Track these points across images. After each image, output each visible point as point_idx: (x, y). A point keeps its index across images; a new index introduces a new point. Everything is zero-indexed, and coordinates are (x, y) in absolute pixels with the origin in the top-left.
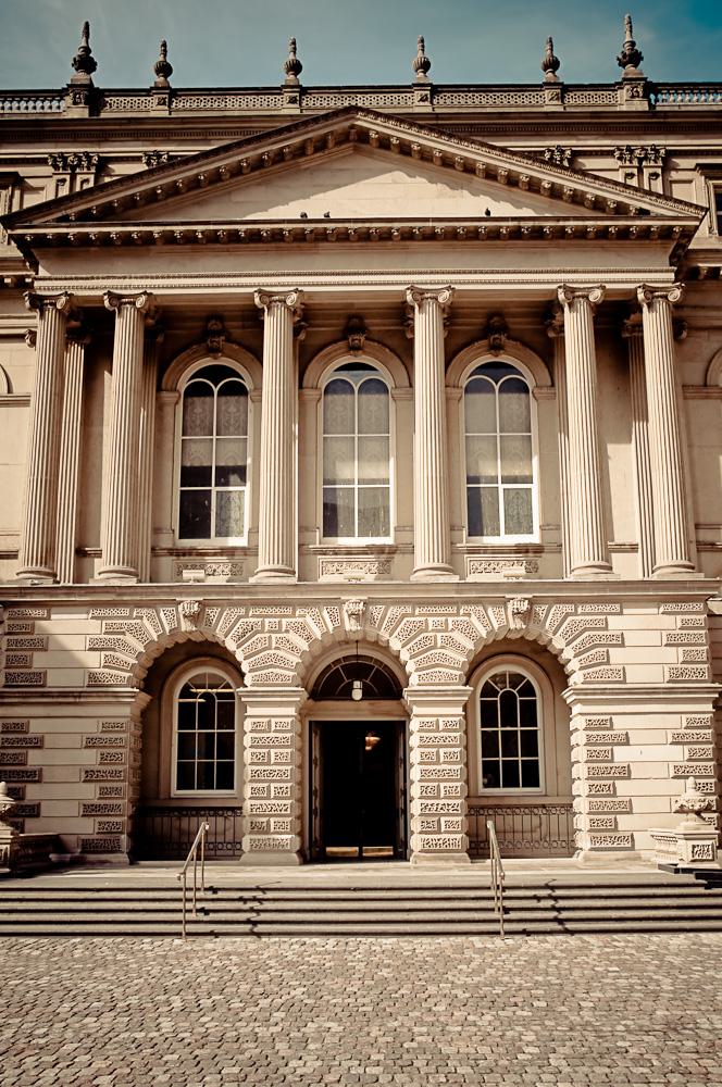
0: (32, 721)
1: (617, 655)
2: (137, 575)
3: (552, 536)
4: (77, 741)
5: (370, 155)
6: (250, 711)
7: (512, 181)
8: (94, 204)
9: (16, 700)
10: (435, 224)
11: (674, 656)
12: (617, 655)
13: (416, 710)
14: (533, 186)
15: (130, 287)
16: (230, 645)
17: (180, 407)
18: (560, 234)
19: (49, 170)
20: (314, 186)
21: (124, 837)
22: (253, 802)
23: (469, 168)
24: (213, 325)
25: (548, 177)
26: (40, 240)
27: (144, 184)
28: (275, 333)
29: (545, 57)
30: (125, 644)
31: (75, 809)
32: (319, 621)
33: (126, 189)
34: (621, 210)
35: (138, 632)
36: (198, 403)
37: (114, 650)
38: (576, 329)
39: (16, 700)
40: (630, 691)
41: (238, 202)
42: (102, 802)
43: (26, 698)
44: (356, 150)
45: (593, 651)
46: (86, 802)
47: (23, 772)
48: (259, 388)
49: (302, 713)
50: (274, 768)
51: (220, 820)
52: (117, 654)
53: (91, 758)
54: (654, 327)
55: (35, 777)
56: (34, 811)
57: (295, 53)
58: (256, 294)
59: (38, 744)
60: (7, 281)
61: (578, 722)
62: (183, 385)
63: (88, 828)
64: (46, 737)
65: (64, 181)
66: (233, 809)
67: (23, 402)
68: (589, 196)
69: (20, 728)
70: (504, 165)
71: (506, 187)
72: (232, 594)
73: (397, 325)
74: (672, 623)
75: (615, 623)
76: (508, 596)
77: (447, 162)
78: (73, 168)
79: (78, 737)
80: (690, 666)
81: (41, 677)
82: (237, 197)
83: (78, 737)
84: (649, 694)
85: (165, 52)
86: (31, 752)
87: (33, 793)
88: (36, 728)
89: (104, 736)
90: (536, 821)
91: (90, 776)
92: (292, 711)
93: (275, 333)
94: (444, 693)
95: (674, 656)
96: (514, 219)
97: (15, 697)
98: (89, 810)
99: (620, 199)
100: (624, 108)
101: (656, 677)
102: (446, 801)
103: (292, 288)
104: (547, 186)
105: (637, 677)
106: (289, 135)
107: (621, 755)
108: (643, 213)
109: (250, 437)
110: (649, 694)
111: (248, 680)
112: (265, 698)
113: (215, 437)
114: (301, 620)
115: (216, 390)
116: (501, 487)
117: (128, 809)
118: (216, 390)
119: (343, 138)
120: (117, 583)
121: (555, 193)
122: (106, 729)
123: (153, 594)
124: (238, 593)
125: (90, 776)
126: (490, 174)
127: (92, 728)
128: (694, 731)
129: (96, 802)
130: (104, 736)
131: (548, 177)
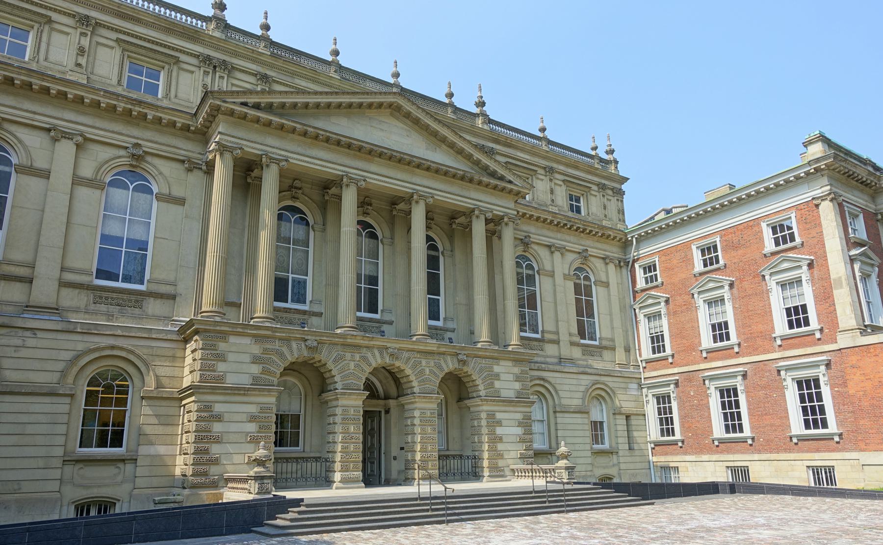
0: (216, 405)
1: (497, 384)
4: (244, 417)
5: (397, 119)
7: (460, 152)
8: (264, 100)
9: (208, 391)
10: (431, 164)
11: (517, 386)
12: (497, 384)
14: (469, 157)
15: (276, 154)
18: (480, 183)
20: (371, 126)
23: (443, 140)
24: (297, 184)
25: (477, 155)
27: (291, 98)
28: (349, 199)
29: (446, 91)
30: (274, 361)
32: (374, 356)
33: (282, 98)
34: (502, 178)
35: (282, 355)
37: (265, 364)
38: (479, 229)
39: (208, 391)
40: (504, 401)
41: (334, 123)
43: (213, 390)
44: (392, 115)
45: (489, 382)
47: (210, 436)
51: (285, 465)
52: (267, 366)
57: (336, 44)
58: (345, 177)
64: (225, 414)
65: (209, 72)
68: (491, 169)
70: (461, 144)
71: (455, 154)
72: (334, 337)
73: (386, 206)
74: (516, 370)
75: (497, 369)
77: (435, 134)
78: (215, 67)
79: (245, 415)
80: (524, 391)
82: (334, 120)
83: (245, 415)
84: (508, 402)
85: (266, 18)
87: (215, 449)
88: (218, 408)
89: (261, 415)
93: (349, 199)
95: (517, 386)
96: (463, 171)
97: (207, 389)
99: (503, 173)
100: (480, 126)
103: (363, 178)
104: (475, 159)
105: (505, 394)
106: (367, 97)
108: (510, 182)
110: (508, 402)
119: (390, 105)
120: (268, 324)
121: (477, 163)
123: (293, 333)
124: (338, 338)
126: (452, 146)
127: (253, 409)
128: (526, 421)
130: (261, 415)
131: (477, 155)
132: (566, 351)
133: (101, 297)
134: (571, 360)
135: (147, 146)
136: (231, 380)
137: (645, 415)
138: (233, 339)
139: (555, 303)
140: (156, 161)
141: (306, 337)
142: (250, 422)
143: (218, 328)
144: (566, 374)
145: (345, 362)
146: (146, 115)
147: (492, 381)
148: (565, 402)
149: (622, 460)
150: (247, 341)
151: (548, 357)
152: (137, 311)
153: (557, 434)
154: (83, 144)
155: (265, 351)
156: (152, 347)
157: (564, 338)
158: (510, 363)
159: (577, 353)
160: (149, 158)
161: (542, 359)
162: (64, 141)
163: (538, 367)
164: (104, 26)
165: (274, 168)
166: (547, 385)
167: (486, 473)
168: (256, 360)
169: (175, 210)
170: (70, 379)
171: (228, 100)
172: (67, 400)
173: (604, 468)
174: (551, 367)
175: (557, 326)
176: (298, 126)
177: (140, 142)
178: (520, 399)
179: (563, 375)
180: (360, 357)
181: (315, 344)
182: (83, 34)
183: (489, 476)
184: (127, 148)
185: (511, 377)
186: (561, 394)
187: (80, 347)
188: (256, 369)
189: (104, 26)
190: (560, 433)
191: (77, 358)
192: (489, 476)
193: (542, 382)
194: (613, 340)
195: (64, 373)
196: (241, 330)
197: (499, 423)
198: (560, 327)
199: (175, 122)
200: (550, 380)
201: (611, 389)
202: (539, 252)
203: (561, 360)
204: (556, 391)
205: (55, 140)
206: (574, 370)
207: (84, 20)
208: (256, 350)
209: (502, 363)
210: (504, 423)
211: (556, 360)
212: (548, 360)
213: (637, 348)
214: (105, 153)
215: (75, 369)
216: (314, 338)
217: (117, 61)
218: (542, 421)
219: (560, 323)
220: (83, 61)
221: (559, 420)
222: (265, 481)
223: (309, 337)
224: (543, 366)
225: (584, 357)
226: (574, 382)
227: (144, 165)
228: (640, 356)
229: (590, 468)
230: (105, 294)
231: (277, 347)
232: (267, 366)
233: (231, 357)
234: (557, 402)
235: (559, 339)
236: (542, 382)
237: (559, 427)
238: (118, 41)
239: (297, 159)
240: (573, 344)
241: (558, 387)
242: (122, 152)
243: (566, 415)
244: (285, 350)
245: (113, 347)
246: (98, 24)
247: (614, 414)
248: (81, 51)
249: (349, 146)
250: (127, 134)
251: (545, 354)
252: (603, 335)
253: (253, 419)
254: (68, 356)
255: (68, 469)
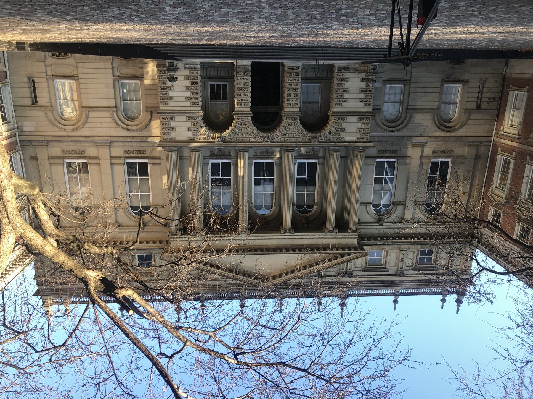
0: (362, 107)
1: (189, 124)
2: (330, 150)
3: (205, 160)
6: (298, 110)
13: (249, 109)
16: (303, 129)
17: (316, 201)
19: (355, 273)
21: (336, 71)
22: (298, 82)
26: (355, 249)
28: (287, 222)
31: (351, 80)
36: (310, 203)
40: (185, 113)
42: (342, 82)
46: (347, 82)
48: (293, 207)
49: (282, 108)
50: (291, 92)
52: (336, 126)
53: (346, 96)
54: (175, 226)
55: (363, 90)
56: (363, 80)
59: (362, 100)
60: (366, 239)
61: (200, 104)
62: (315, 207)
63: (347, 75)
65: (349, 270)
66: (303, 79)
67: (362, 204)
69: (366, 105)
74: (173, 134)
76: (222, 143)
78: (346, 273)
81: (360, 120)
84: (181, 113)
86: (363, 98)
88: (361, 105)
90: (211, 73)
91: (346, 90)
92: (286, 110)
93: (287, 222)
94: (241, 114)
98: (347, 80)
101: (178, 118)
102: (240, 81)
105: (183, 118)
107: (188, 94)
109: (295, 192)
110: (181, 113)
111: (299, 118)
112: (293, 113)
113: (306, 192)
114: (283, 137)
115: (305, 206)
116: (221, 177)
117: (335, 81)
118: (305, 206)
120: (336, 148)
122: (341, 104)
125: (346, 90)
127: (345, 105)
129: (344, 82)
132: (104, 153)
133: (395, 153)
134: (98, 145)
135: (377, 226)
136: (354, 119)
137: (14, 106)
138: (354, 139)
139: (113, 186)
140: (371, 220)
141: (318, 143)
142: (346, 99)
143: (362, 143)
144: (105, 135)
145: (295, 132)
146: (380, 240)
147: (194, 126)
148: (107, 114)
149: (43, 70)
150: (347, 139)
151: (121, 146)
152: (381, 149)
153: (115, 91)
154: (402, 220)
155: (338, 134)
156: (377, 132)
157: (106, 163)
158: (178, 139)
159: (92, 151)
160: (375, 221)
161: (126, 144)
162: (409, 219)
163: (133, 138)
164: (393, 275)
165: (331, 228)
166: (125, 126)
167: (199, 66)
168: (343, 129)
169: (365, 200)
170: (408, 116)
171: (358, 254)
172: (409, 107)
173: (62, 64)
174: (117, 139)
175: (112, 169)
176: (323, 252)
177: (380, 227)
178: (170, 115)
179: (108, 134)
180: (287, 135)
181: (313, 140)
182: (401, 268)
183: (197, 65)
184: (385, 223)
185: (177, 129)
186: (110, 120)
187: (404, 130)
188: (344, 125)
189: (393, 275)
190: (112, 91)
191: (406, 125)
192: (197, 65)
193: (129, 128)
194: (50, 164)
195: (411, 118)
196: (352, 143)
197: (188, 99)
198: (110, 169)
199: (368, 240)
200: (121, 130)
201: (56, 126)
202: (128, 220)
203: (110, 145)
204: (115, 121)
205: (412, 219)
206: (97, 139)
207: (401, 274)
208: (343, 135)
209: (185, 139)
210: (184, 99)
211: (113, 144)
212: (121, 144)
213: (23, 161)
214: (392, 219)
215: (406, 121)
216: (314, 143)
217: (388, 261)
218: (123, 100)
219: (110, 171)
220: (402, 256)
221: (113, 101)
222: (373, 71)
223: (317, 143)
224: (129, 140)
225: (83, 149)
226: (97, 129)
227: (377, 217)
228: (20, 153)
229: (79, 65)
230: (393, 155)
231: (332, 137)
232: (338, 127)
233: (355, 130)
234: (115, 114)
235: (110, 160)
236: (129, 128)
237: (113, 96)
238: (388, 271)
239: (319, 235)
240: (98, 158)
241: (114, 125)
242: (386, 220)
243: (106, 105)
244: (328, 135)
245: (393, 131)
246: (395, 275)
247: (51, 106)
248: (402, 261)
249: (287, 250)
250: (386, 229)
251: (124, 148)
252: (62, 166)
253: (345, 100)
254: (409, 126)
255: (408, 77)
